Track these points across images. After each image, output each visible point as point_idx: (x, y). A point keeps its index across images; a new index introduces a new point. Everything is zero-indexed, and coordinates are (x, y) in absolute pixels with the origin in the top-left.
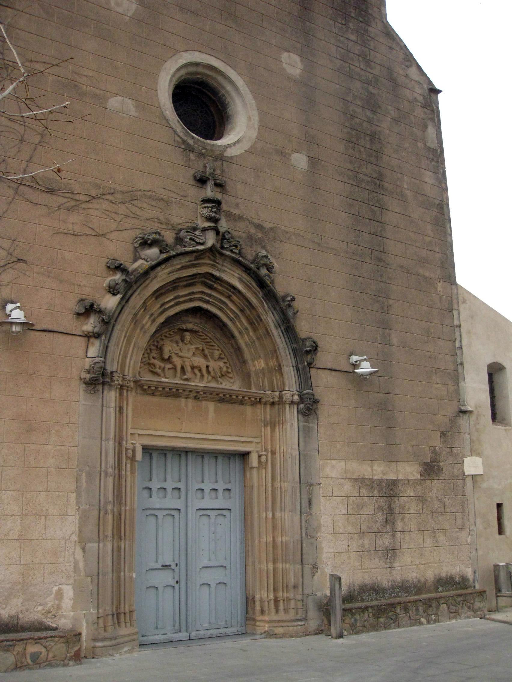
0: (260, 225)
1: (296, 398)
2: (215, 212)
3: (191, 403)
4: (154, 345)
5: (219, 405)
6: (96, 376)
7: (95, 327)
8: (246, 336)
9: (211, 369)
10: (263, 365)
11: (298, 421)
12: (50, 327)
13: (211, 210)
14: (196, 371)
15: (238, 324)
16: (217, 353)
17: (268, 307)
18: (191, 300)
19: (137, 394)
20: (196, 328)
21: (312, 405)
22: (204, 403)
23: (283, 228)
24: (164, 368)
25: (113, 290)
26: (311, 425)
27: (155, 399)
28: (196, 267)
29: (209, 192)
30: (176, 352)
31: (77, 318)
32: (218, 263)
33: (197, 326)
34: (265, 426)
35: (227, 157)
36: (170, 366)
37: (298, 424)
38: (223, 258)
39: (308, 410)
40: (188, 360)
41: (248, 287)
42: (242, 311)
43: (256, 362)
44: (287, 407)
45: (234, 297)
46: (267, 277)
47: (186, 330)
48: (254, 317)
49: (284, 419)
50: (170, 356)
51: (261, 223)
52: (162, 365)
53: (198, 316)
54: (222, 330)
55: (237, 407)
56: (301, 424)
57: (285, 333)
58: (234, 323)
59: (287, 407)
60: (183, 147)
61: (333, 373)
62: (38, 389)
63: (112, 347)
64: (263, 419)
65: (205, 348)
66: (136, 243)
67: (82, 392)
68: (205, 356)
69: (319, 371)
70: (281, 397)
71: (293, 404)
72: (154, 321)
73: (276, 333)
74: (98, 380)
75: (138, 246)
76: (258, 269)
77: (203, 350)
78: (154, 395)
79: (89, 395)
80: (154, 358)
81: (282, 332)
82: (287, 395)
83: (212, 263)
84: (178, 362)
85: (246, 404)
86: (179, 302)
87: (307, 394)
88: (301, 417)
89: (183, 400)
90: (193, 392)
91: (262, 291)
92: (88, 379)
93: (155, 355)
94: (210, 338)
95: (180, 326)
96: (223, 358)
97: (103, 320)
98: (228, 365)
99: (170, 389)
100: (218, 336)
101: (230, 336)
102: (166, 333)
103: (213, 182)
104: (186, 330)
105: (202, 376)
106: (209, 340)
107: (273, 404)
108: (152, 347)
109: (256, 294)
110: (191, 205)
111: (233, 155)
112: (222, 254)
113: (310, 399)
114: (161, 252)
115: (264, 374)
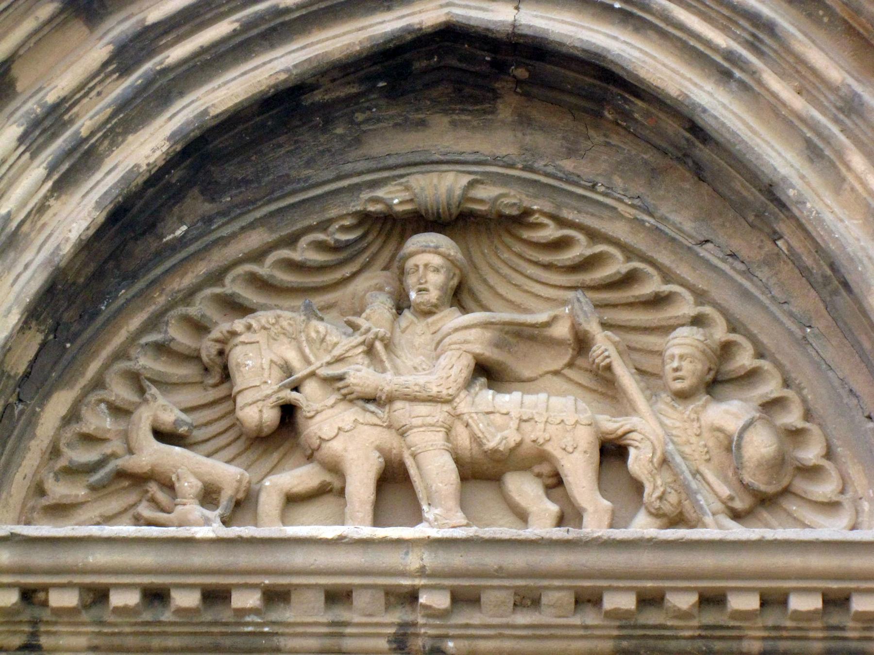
4: (162, 349)
9: (638, 461)
14: (525, 489)
16: (683, 349)
33: (505, 180)
36: (299, 477)
40: (439, 413)
50: (288, 411)
52: (228, 473)
53: (505, 112)
54: (699, 172)
58: (750, 91)
65: (593, 327)
68: (605, 383)
77: (582, 343)
80: (162, 435)
84: (350, 438)
90: (361, 600)
94: (629, 252)
95: (362, 202)
96: (751, 376)
98: (793, 418)
99: (156, 596)
100: (683, 220)
101: (752, 194)
102: (258, 256)
106: (618, 266)
108: (146, 362)
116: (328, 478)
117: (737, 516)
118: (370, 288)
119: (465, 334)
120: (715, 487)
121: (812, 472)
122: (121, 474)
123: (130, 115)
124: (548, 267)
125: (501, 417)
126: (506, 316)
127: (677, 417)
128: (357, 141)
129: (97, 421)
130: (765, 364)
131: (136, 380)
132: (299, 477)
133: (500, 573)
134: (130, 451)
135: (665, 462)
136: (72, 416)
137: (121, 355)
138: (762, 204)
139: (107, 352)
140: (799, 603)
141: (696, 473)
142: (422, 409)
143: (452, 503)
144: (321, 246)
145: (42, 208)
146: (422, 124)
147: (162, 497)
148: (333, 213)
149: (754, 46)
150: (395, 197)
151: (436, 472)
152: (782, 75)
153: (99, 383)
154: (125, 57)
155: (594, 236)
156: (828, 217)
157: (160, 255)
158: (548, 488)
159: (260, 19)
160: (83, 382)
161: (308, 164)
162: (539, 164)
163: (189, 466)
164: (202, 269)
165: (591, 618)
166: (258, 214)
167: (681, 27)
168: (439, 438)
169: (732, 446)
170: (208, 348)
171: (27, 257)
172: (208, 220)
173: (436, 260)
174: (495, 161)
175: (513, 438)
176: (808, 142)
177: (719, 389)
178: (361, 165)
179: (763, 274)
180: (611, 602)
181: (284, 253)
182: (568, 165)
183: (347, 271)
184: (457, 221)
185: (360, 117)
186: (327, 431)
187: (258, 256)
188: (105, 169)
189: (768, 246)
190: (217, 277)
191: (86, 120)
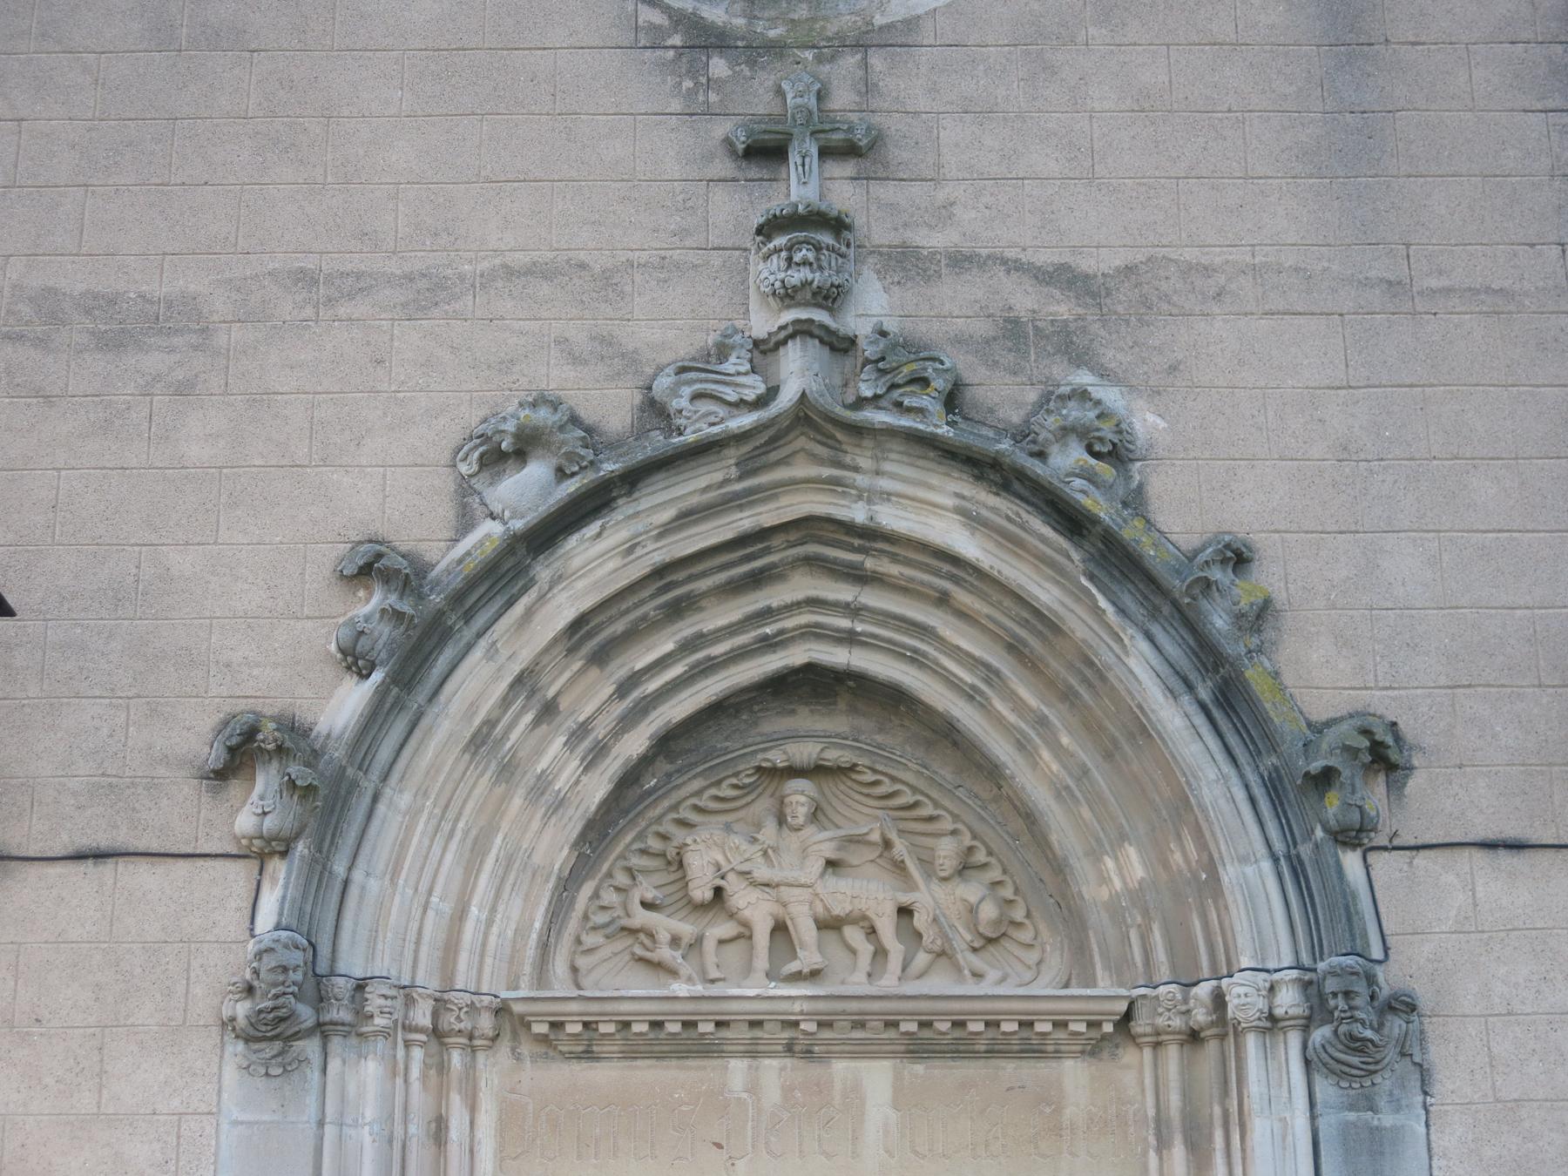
0: (1064, 268)
1: (1288, 1000)
2: (805, 263)
3: (774, 1072)
4: (644, 852)
5: (919, 1068)
6: (270, 1004)
7: (265, 814)
8: (1046, 754)
9: (920, 921)
10: (1138, 871)
12: (103, 841)
13: (789, 259)
14: (854, 935)
15: (1000, 706)
16: (947, 851)
17: (1122, 611)
18: (768, 644)
19: (518, 1058)
20: (833, 756)
22: (840, 1067)
23: (1190, 254)
24: (697, 943)
25: (355, 661)
26: (1387, 1119)
27: (604, 1075)
28: (751, 504)
29: (800, 185)
30: (745, 867)
31: (214, 791)
32: (856, 469)
33: (844, 747)
34: (1163, 1144)
35: (890, 27)
36: (726, 929)
38: (867, 443)
40: (805, 894)
41: (1011, 541)
42: (1014, 648)
43: (1109, 863)
45: (962, 597)
46: (1078, 483)
47: (793, 772)
48: (1070, 666)
50: (718, 891)
51: (1067, 258)
52: (686, 928)
53: (842, 705)
55: (1011, 1070)
56: (1327, 1124)
57: (1217, 714)
58: (985, 708)
59: (1251, 1042)
60: (677, 40)
61: (1505, 859)
62: (49, 1080)
63: (374, 885)
64: (1151, 1112)
66: (464, 459)
67: (231, 1074)
68: (899, 867)
69: (1421, 859)
72: (599, 752)
73: (1174, 719)
74: (294, 1012)
75: (475, 468)
76: (1041, 455)
77: (887, 844)
78: (598, 1059)
79: (261, 1083)
80: (646, 905)
81: (1203, 707)
83: (826, 472)
84: (756, 909)
85: (1058, 1055)
86: (710, 658)
87: (1332, 973)
88: (1325, 1089)
89: (738, 1067)
90: (767, 1026)
91: (1078, 546)
92: (241, 1022)
93: (650, 895)
94: (915, 790)
95: (759, 760)
97: (292, 784)
98: (1008, 892)
99: (657, 1025)
100: (946, 774)
102: (699, 793)
103: (814, 151)
104: (793, 772)
105: (880, 953)
106: (908, 798)
107: (1194, 1037)
108: (636, 861)
109: (1052, 564)
110: (716, 259)
111: (920, 11)
112: (858, 431)
114: (561, 474)
115: (1146, 913)
116: (742, 929)
117: (975, 950)
118: (763, 805)
119: (823, 843)
120: (962, 937)
121: (1018, 925)
122: (623, 929)
123: (627, 722)
124: (868, 795)
125: (842, 894)
126: (842, 833)
127: (939, 891)
128: (756, 724)
129: (609, 897)
130: (993, 860)
131: (629, 871)
132: (726, 929)
133: (844, 1013)
134: (628, 916)
135: (935, 920)
136: (596, 895)
137: (622, 856)
138: (991, 771)
139: (612, 857)
140: (1006, 1027)
141: (952, 926)
142: (797, 891)
143: (814, 948)
144: (735, 786)
145: (577, 782)
146: (793, 712)
147: (647, 941)
148: (741, 768)
149: (987, 681)
150: (777, 758)
151: (805, 930)
152: (1003, 699)
153: (609, 875)
154: (622, 690)
155: (893, 779)
156: (1028, 787)
157: (643, 797)
158: (868, 934)
159: (698, 663)
160: (600, 875)
161: (726, 739)
162: (863, 737)
163: (664, 924)
164: (666, 803)
165: (892, 1034)
166: (699, 770)
167: (945, 669)
168: (806, 908)
169: (973, 910)
170: (671, 853)
171: (571, 811)
172: (669, 775)
173: (803, 799)
174: (837, 736)
175: (848, 908)
176: (1018, 741)
177: (967, 872)
178: (759, 739)
179: (992, 807)
180: (904, 1027)
181: (713, 791)
182: (879, 738)
183: (749, 798)
184: (816, 771)
185: (756, 708)
186: (741, 904)
187: (699, 793)
188: (612, 755)
189: (995, 790)
190: (675, 807)
191: (600, 730)
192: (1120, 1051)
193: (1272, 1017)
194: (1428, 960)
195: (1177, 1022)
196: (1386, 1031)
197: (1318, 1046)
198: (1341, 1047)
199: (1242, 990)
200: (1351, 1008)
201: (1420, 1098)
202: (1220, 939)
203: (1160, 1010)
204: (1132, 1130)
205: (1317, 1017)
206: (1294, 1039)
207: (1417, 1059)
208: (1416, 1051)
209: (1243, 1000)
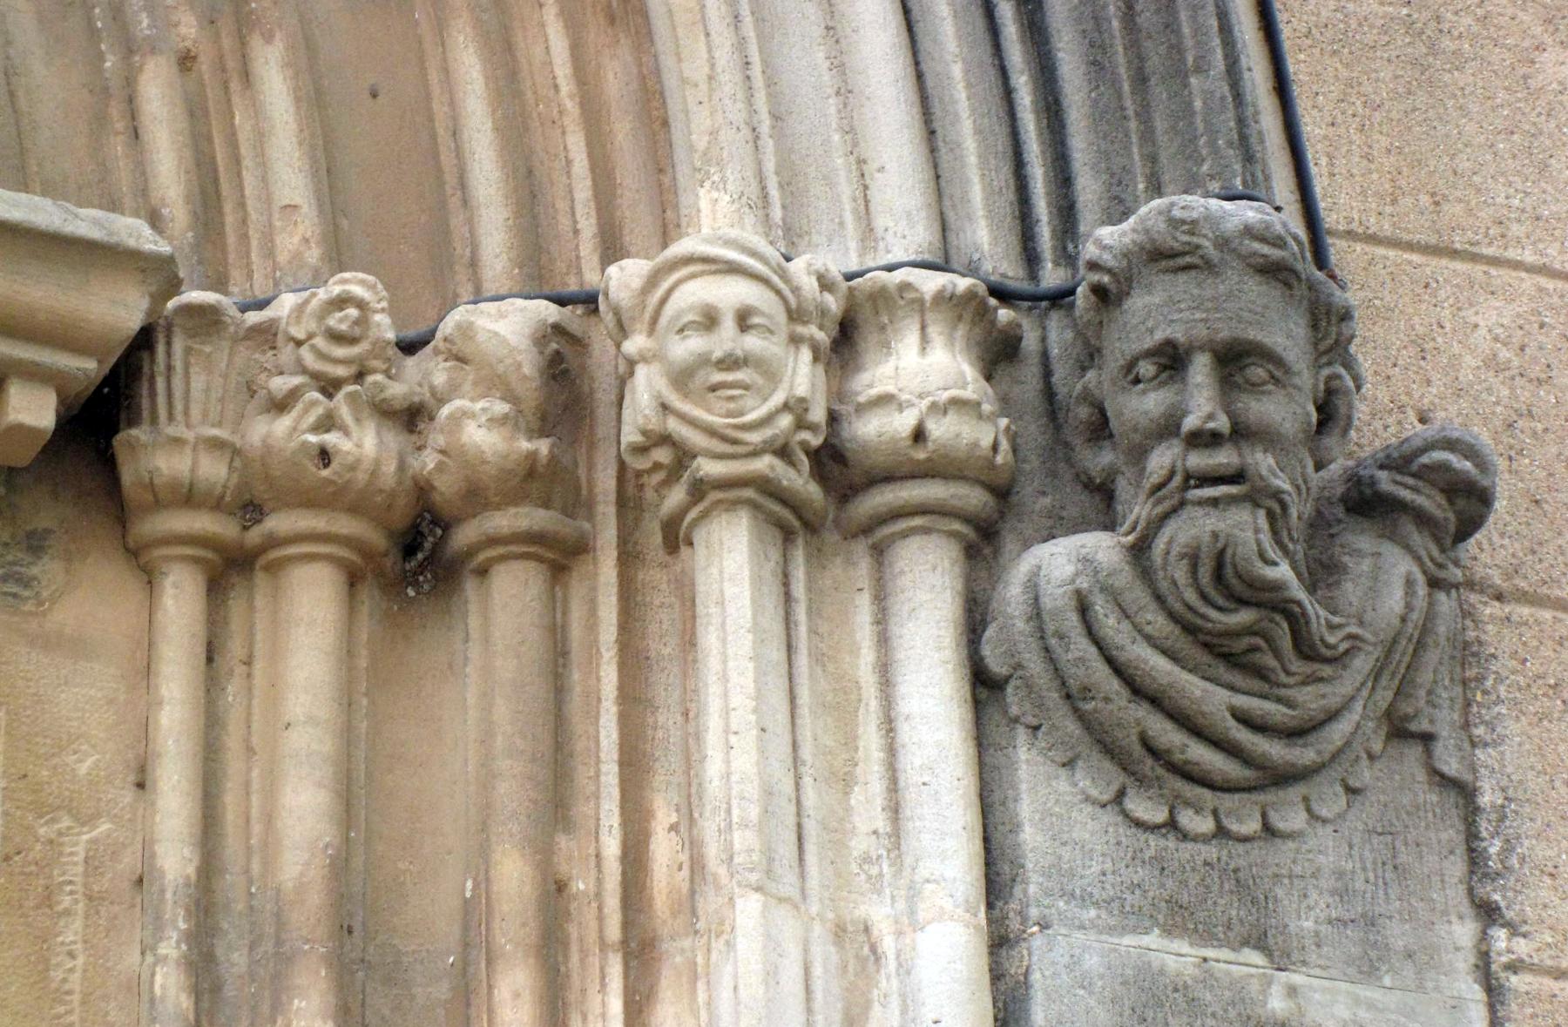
1: (921, 379)
11: (997, 878)
21: (1322, 572)
37: (1000, 942)
39: (1225, 654)
44: (730, 562)
49: (663, 849)
59: (730, 562)
64: (176, 860)
70: (565, 387)
71: (877, 536)
82: (701, 314)
87: (1164, 256)
88: (1060, 810)
113: (1234, 359)
192: (48, 570)
193: (833, 461)
194: (1492, 363)
195: (364, 444)
196: (1351, 592)
197: (1056, 596)
198: (1157, 622)
199: (730, 293)
200: (1241, 433)
201: (1464, 931)
202: (576, 144)
203: (280, 384)
204: (72, 933)
205: (1035, 499)
206: (928, 582)
207: (1451, 766)
208: (1444, 722)
209: (726, 339)
